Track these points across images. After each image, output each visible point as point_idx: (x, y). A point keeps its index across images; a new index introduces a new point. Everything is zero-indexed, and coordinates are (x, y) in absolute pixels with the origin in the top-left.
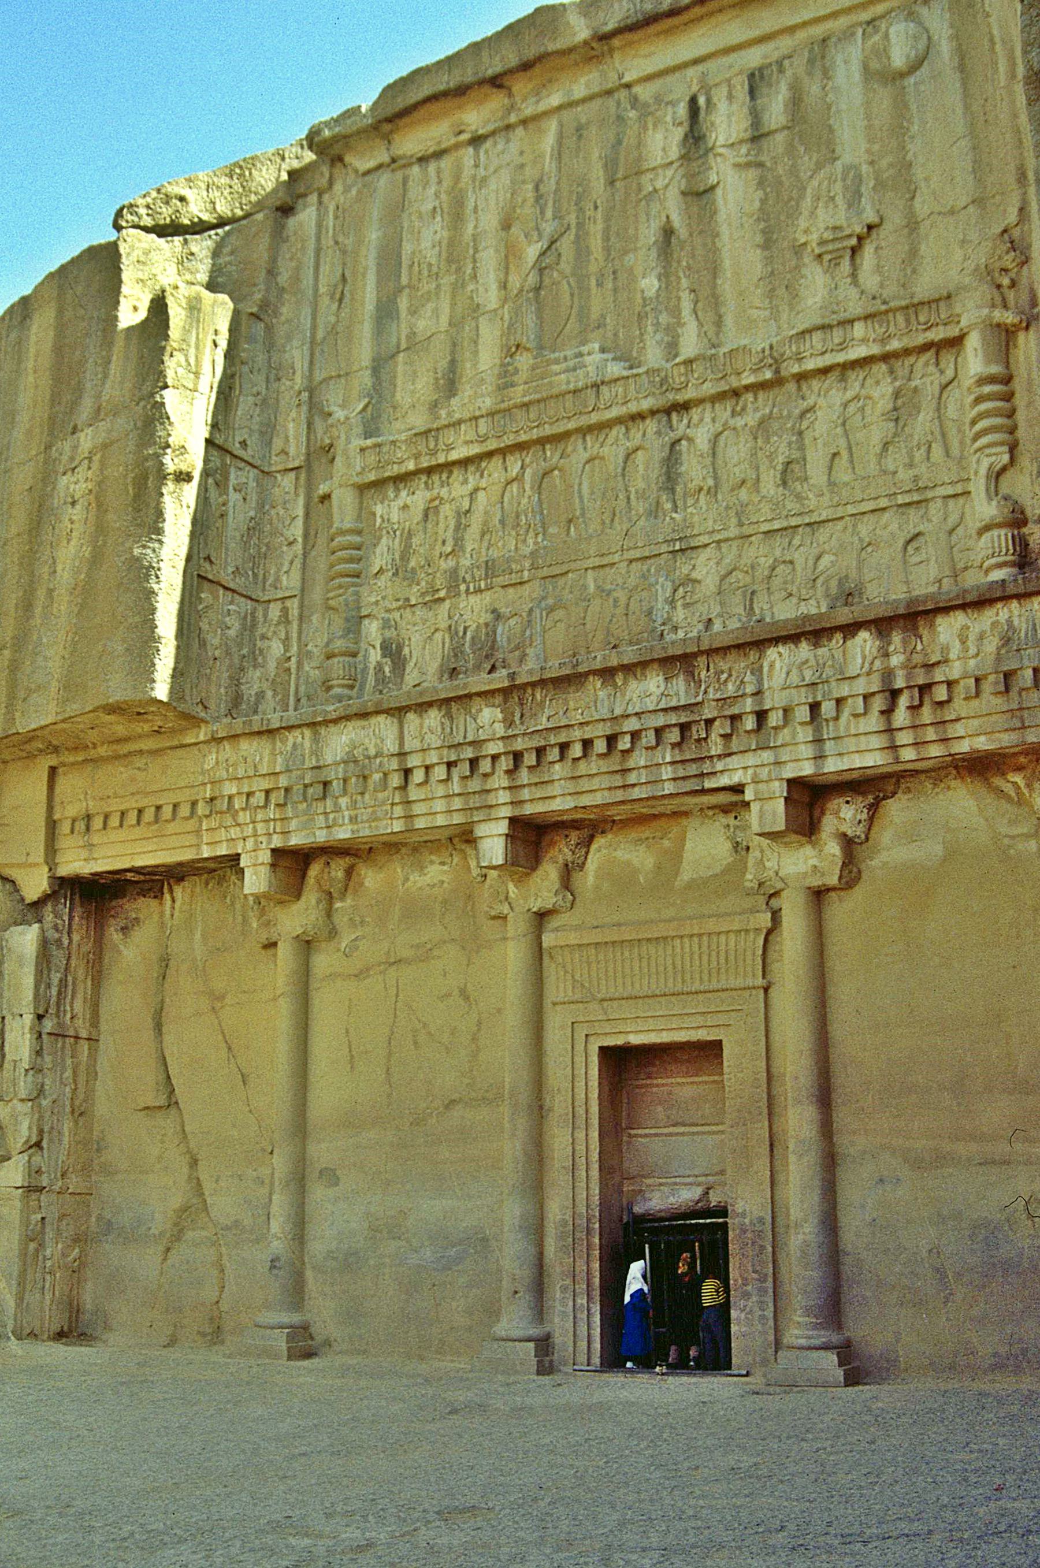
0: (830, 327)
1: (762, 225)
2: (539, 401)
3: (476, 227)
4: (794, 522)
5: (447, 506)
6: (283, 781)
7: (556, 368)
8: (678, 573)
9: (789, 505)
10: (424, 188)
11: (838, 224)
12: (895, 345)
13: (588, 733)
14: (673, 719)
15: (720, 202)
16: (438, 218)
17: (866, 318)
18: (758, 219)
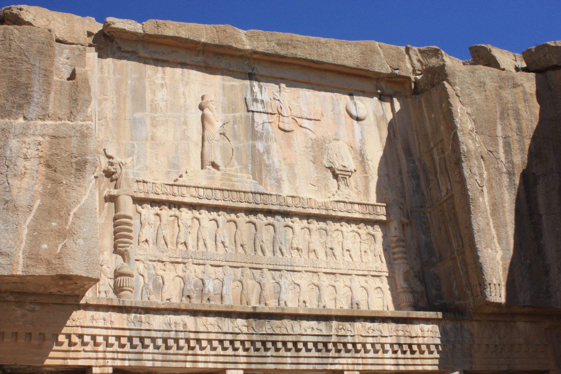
0: (346, 202)
1: (312, 154)
2: (228, 191)
3: (185, 102)
4: (334, 271)
5: (180, 221)
6: (127, 333)
7: (233, 179)
8: (289, 279)
9: (332, 265)
10: (156, 73)
11: (345, 165)
12: (368, 217)
13: (286, 338)
14: (321, 339)
15: (295, 138)
16: (165, 89)
17: (359, 204)
18: (311, 151)
